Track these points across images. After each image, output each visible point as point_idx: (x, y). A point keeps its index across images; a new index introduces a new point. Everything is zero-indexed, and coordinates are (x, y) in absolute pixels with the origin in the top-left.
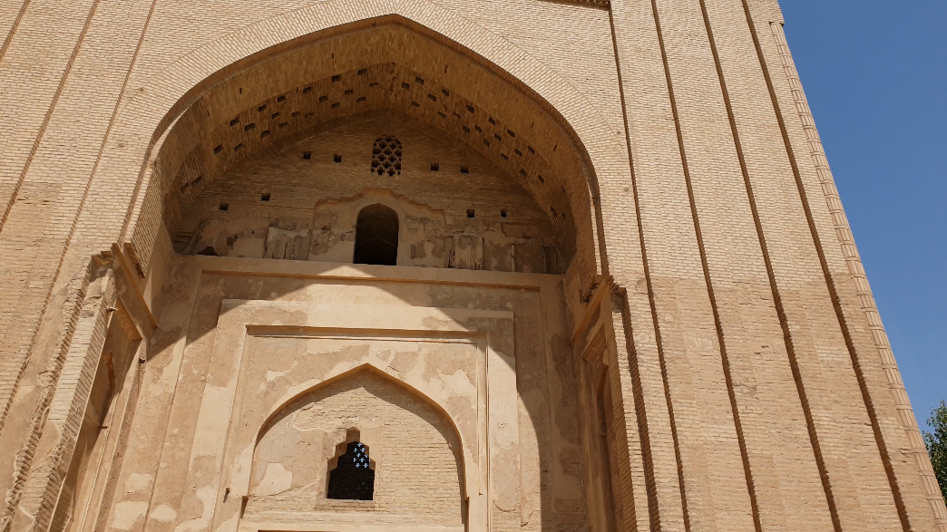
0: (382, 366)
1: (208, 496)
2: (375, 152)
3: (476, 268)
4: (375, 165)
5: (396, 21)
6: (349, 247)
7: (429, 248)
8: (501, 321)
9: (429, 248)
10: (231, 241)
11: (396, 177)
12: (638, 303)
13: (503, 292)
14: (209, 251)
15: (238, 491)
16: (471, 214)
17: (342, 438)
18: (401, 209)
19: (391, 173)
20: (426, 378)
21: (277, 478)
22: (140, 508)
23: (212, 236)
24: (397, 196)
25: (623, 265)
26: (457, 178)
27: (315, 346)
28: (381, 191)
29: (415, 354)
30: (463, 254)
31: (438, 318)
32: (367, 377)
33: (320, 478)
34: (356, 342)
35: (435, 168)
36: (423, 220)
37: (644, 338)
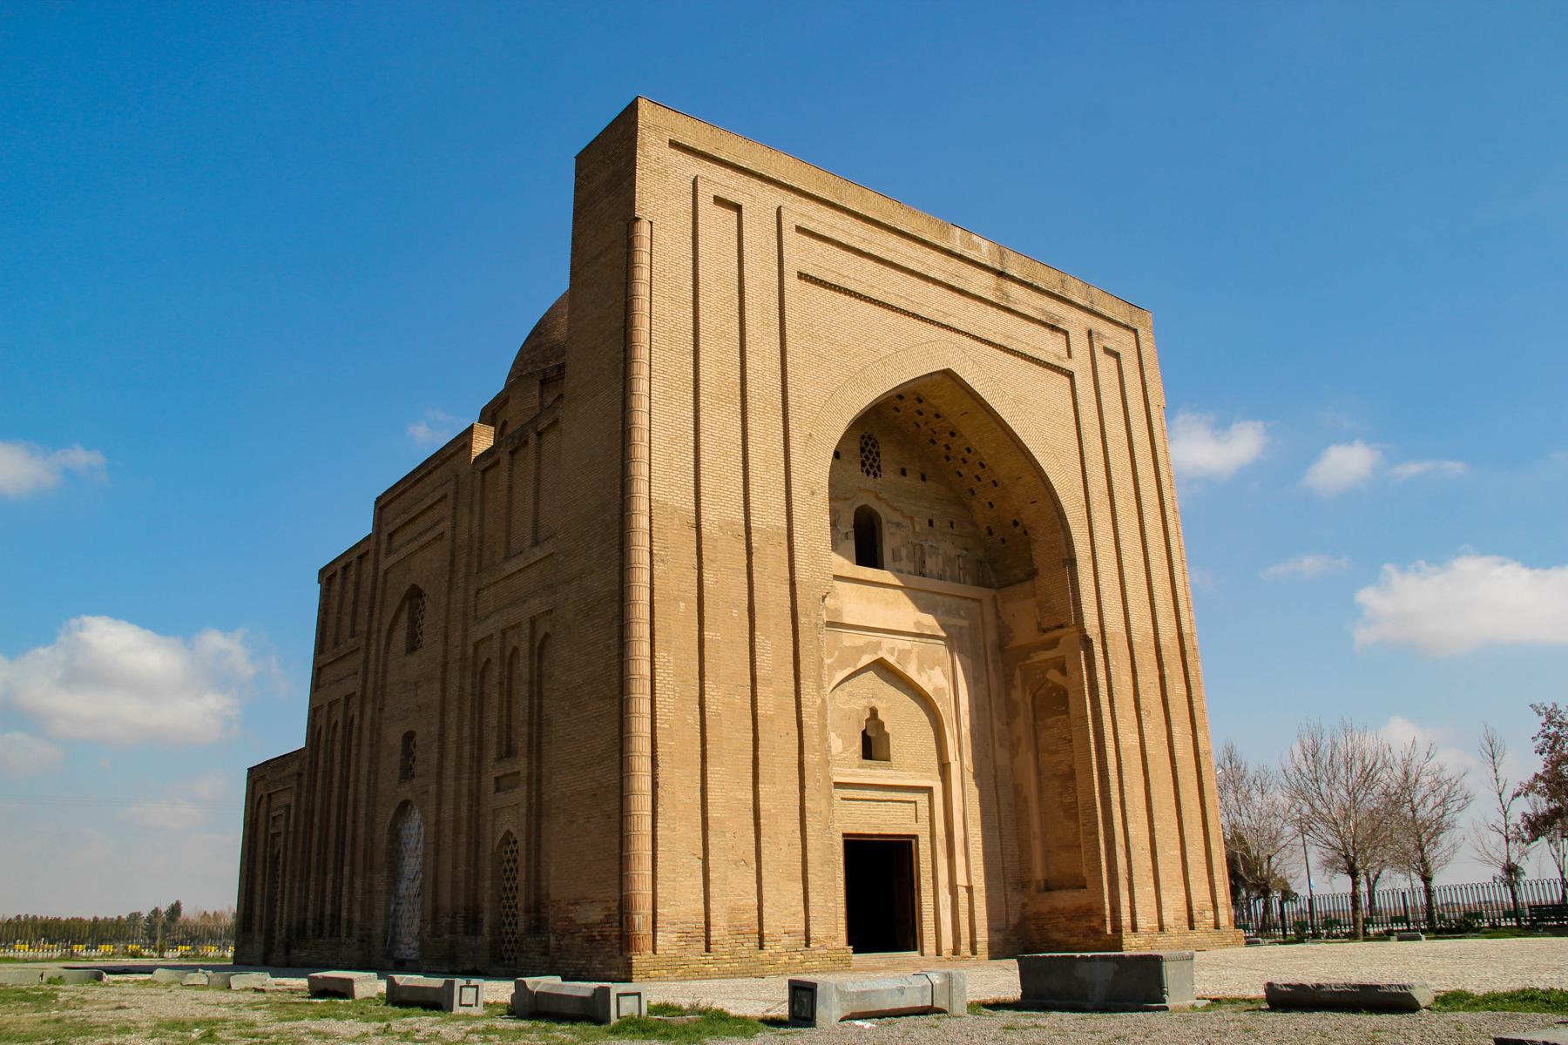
0: (891, 660)
2: (862, 450)
3: (940, 578)
4: (863, 464)
5: (948, 373)
7: (904, 552)
8: (961, 628)
9: (904, 552)
11: (879, 480)
12: (1097, 648)
13: (958, 600)
16: (931, 523)
18: (884, 512)
19: (875, 475)
20: (919, 672)
24: (879, 499)
26: (919, 484)
27: (850, 639)
29: (910, 652)
30: (932, 564)
31: (929, 622)
32: (882, 668)
34: (873, 638)
35: (903, 473)
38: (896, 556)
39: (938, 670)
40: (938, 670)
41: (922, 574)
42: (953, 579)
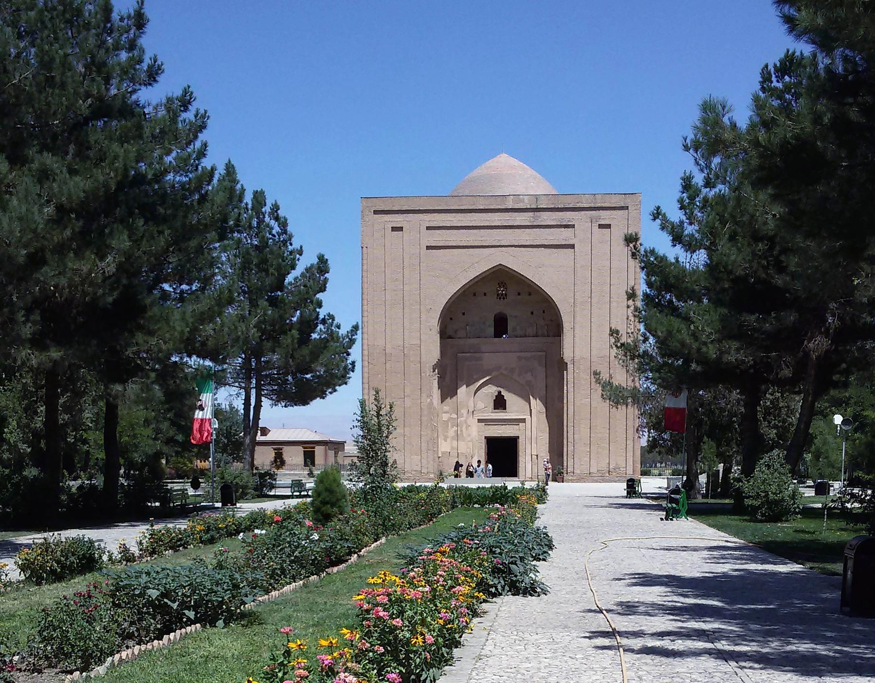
1: (464, 412)
6: (491, 330)
10: (456, 332)
12: (570, 366)
14: (450, 337)
15: (471, 410)
16: (532, 313)
17: (497, 393)
18: (509, 312)
21: (481, 405)
22: (448, 415)
23: (450, 332)
25: (567, 354)
28: (500, 307)
33: (492, 404)
35: (519, 294)
36: (516, 317)
37: (570, 377)
38: (514, 329)
39: (529, 374)
40: (529, 374)
41: (526, 336)
42: (543, 336)
